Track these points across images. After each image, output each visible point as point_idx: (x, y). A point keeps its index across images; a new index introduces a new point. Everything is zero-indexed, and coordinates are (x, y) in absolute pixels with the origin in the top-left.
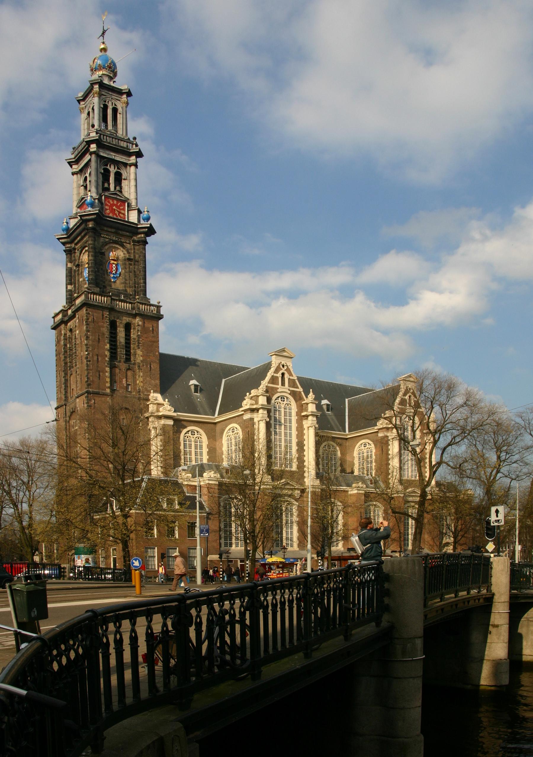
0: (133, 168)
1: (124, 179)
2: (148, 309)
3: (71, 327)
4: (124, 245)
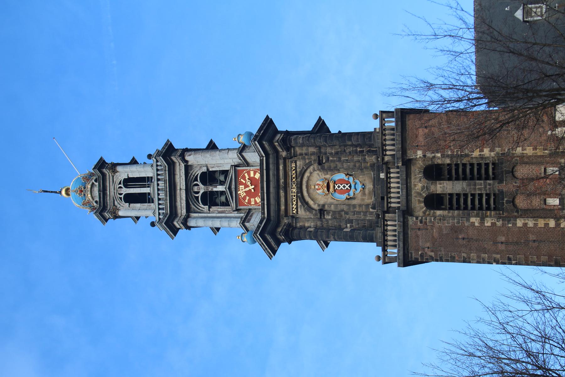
1: (208, 169)
2: (392, 137)
4: (301, 171)
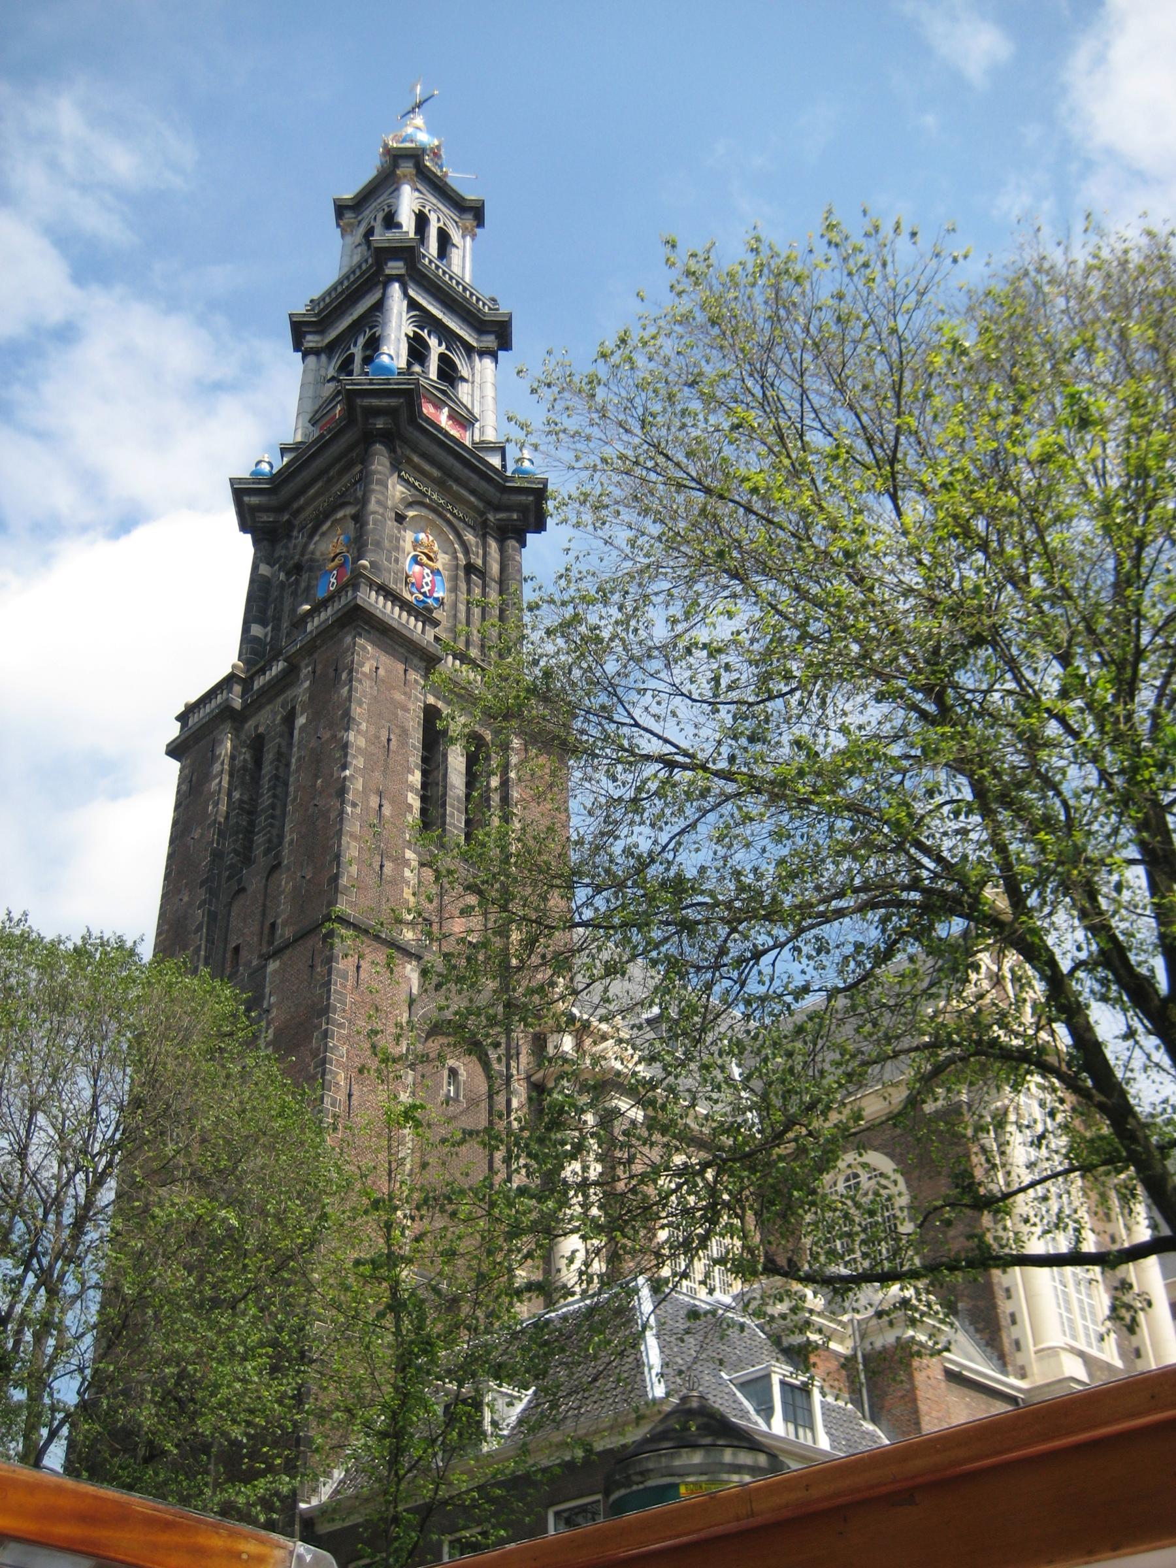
0: (488, 362)
3: (261, 730)
